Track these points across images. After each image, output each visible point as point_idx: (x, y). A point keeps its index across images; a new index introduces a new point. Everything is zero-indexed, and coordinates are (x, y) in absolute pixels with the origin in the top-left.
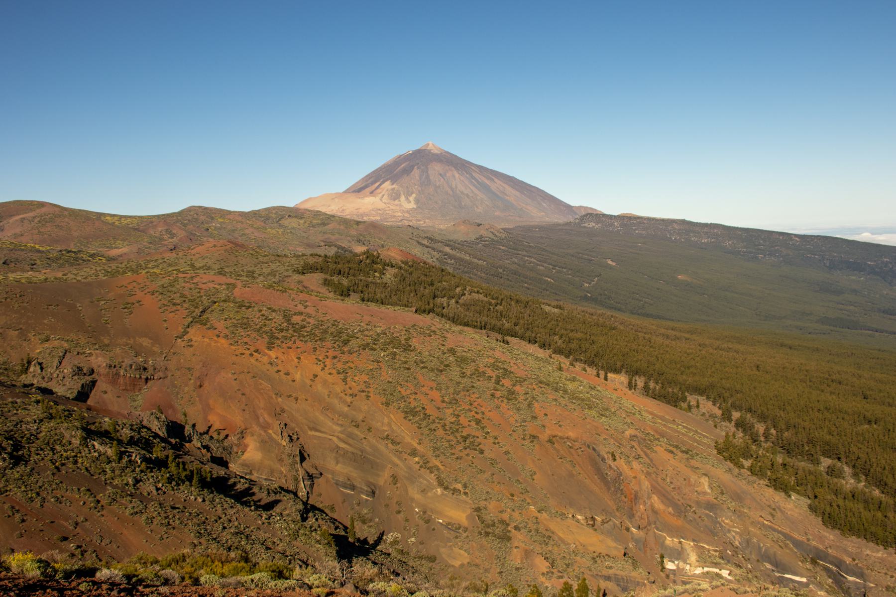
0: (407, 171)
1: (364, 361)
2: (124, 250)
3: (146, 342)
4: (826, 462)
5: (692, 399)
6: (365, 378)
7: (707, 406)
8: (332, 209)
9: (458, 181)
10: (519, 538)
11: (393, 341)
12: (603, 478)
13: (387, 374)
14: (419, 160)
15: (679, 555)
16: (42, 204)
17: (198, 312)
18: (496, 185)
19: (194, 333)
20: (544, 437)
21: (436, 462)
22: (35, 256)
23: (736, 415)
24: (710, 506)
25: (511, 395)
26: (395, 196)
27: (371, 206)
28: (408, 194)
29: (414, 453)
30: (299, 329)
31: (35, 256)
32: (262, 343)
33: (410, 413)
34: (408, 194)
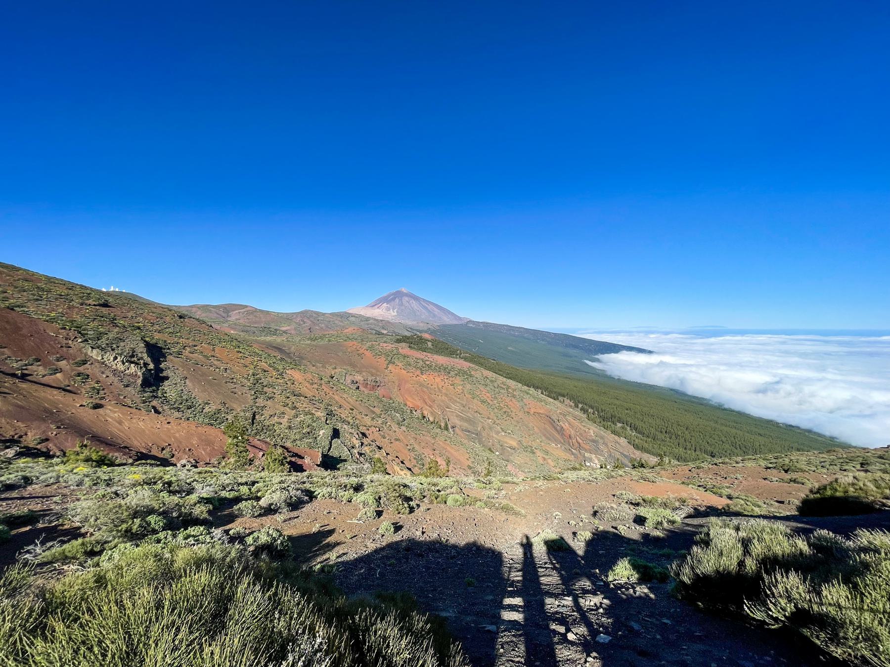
0: (394, 299)
1: (458, 380)
2: (288, 328)
3: (374, 371)
4: (619, 425)
5: (561, 398)
6: (460, 387)
7: (567, 401)
8: (362, 313)
9: (414, 304)
10: (538, 453)
11: (465, 373)
12: (556, 429)
13: (468, 386)
14: (399, 295)
15: (590, 460)
16: (247, 306)
17: (389, 358)
18: (430, 307)
19: (390, 366)
20: (532, 413)
21: (497, 422)
22: (255, 329)
23: (580, 406)
24: (594, 441)
25: (514, 396)
26: (388, 309)
27: (378, 313)
28: (393, 309)
29: (489, 418)
30: (430, 367)
31: (255, 329)
32: (418, 372)
33: (483, 402)
34: (393, 309)
